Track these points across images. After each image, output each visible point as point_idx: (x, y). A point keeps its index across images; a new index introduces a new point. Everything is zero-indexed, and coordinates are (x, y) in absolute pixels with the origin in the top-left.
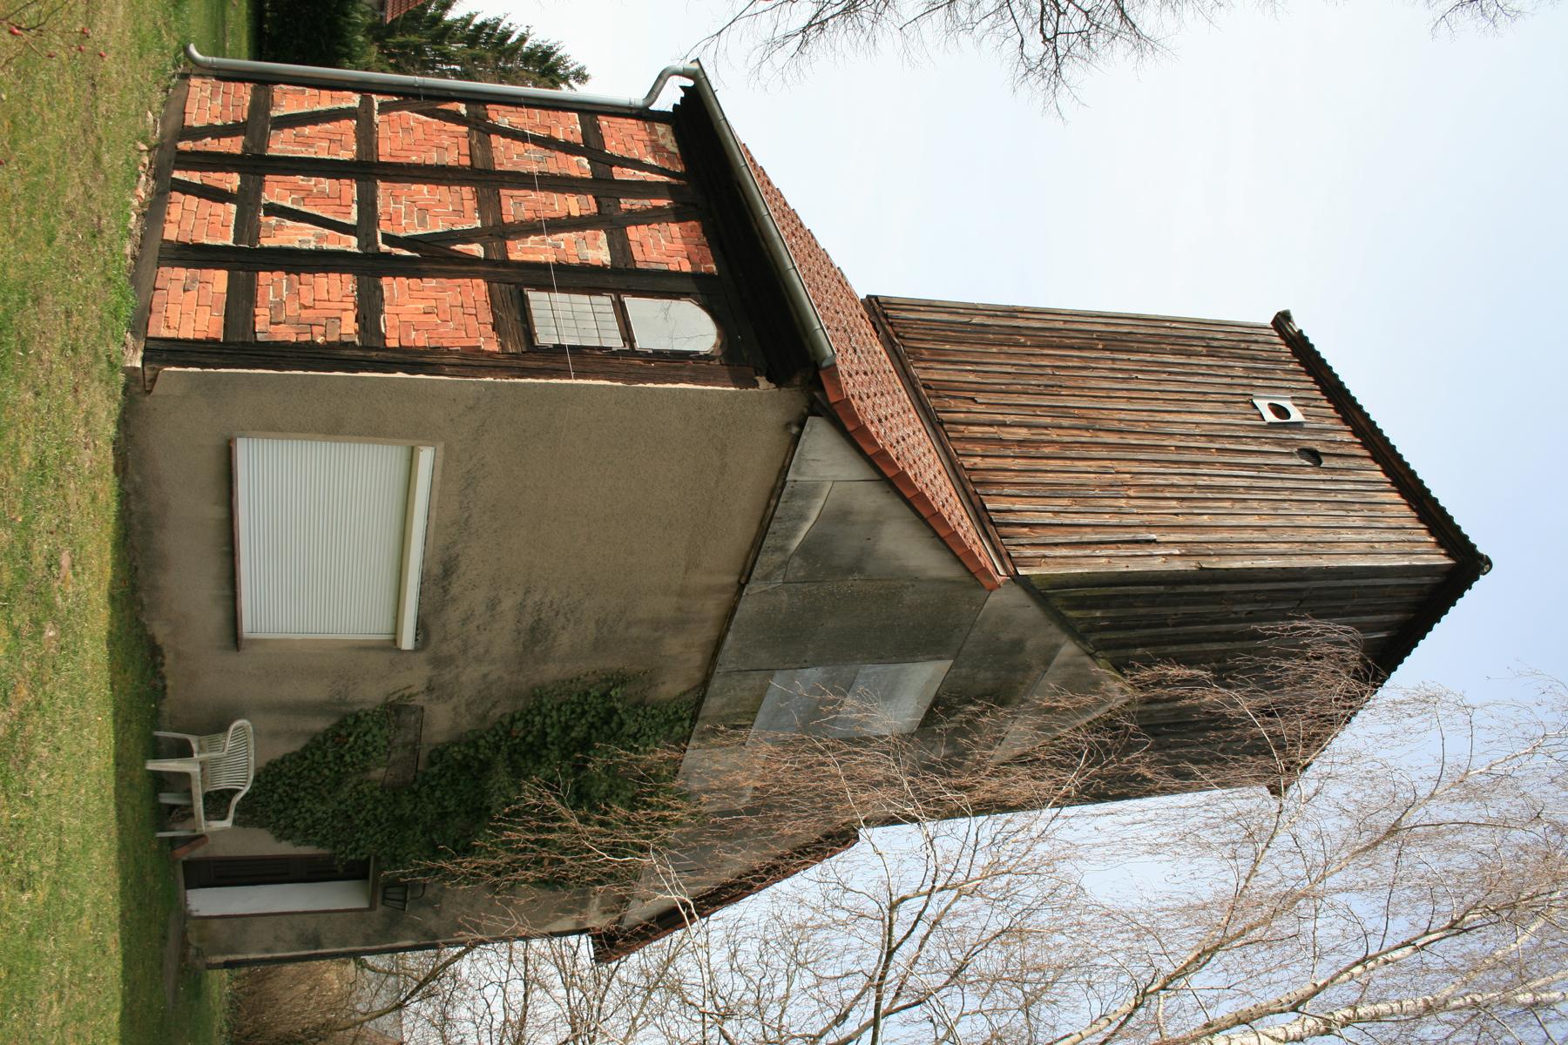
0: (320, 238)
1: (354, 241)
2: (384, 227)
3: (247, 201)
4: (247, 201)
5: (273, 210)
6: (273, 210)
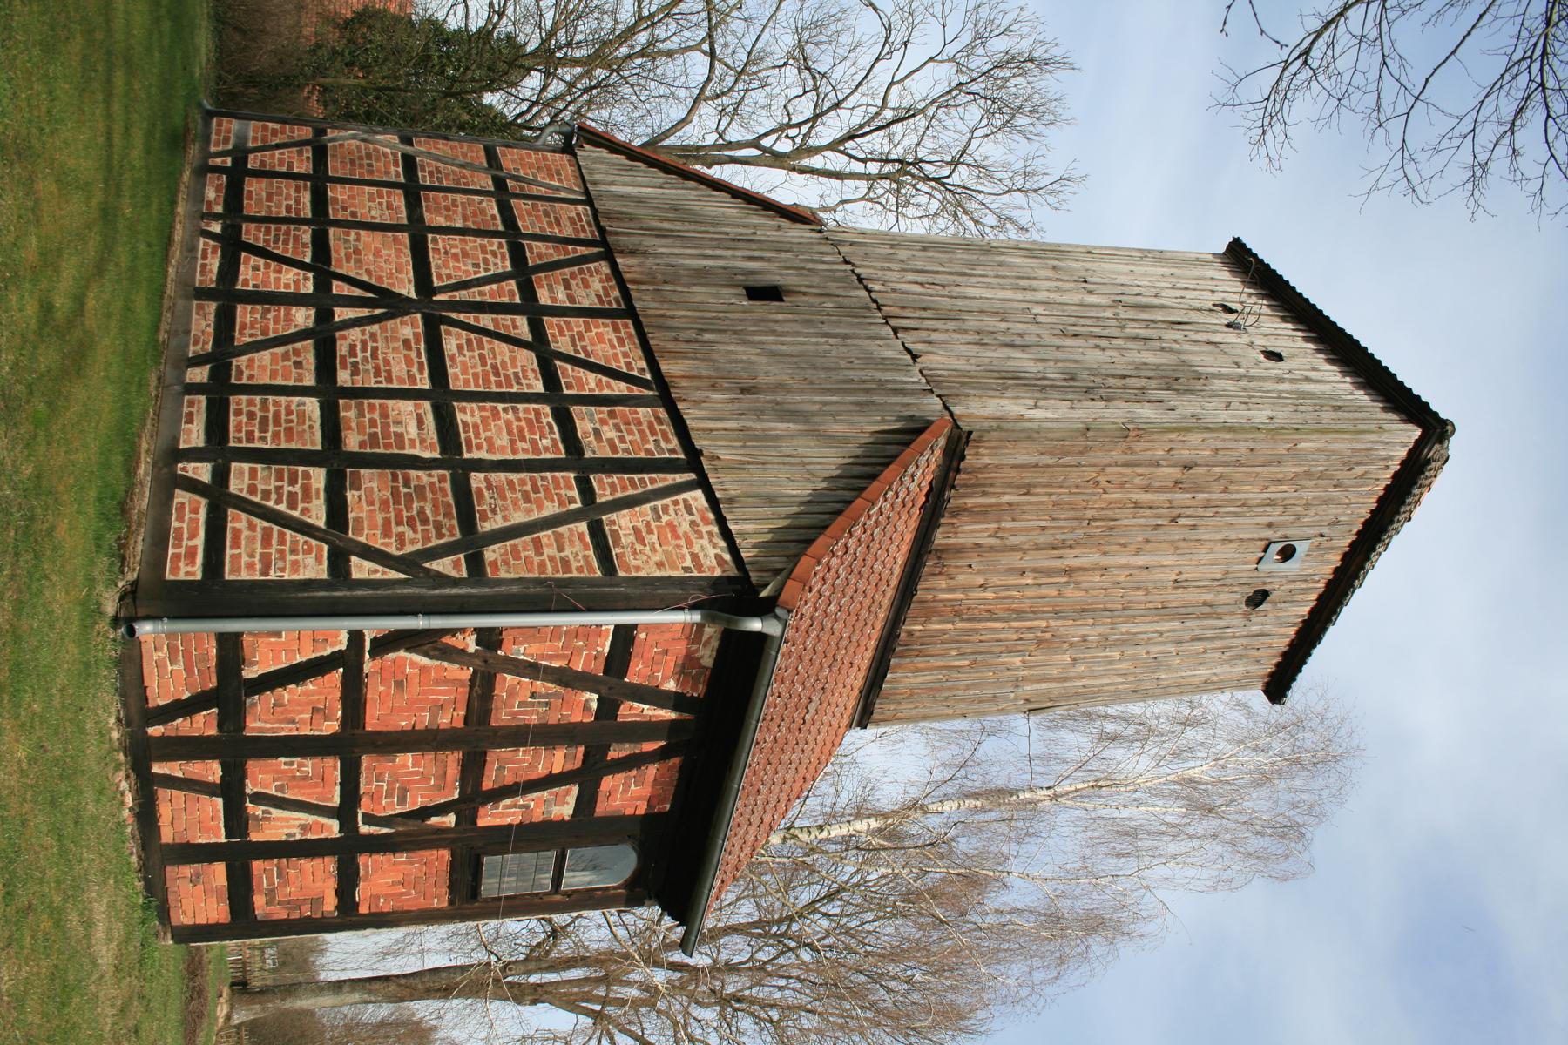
0: (305, 828)
1: (335, 825)
2: (365, 806)
3: (231, 791)
4: (231, 791)
5: (259, 798)
6: (259, 798)
